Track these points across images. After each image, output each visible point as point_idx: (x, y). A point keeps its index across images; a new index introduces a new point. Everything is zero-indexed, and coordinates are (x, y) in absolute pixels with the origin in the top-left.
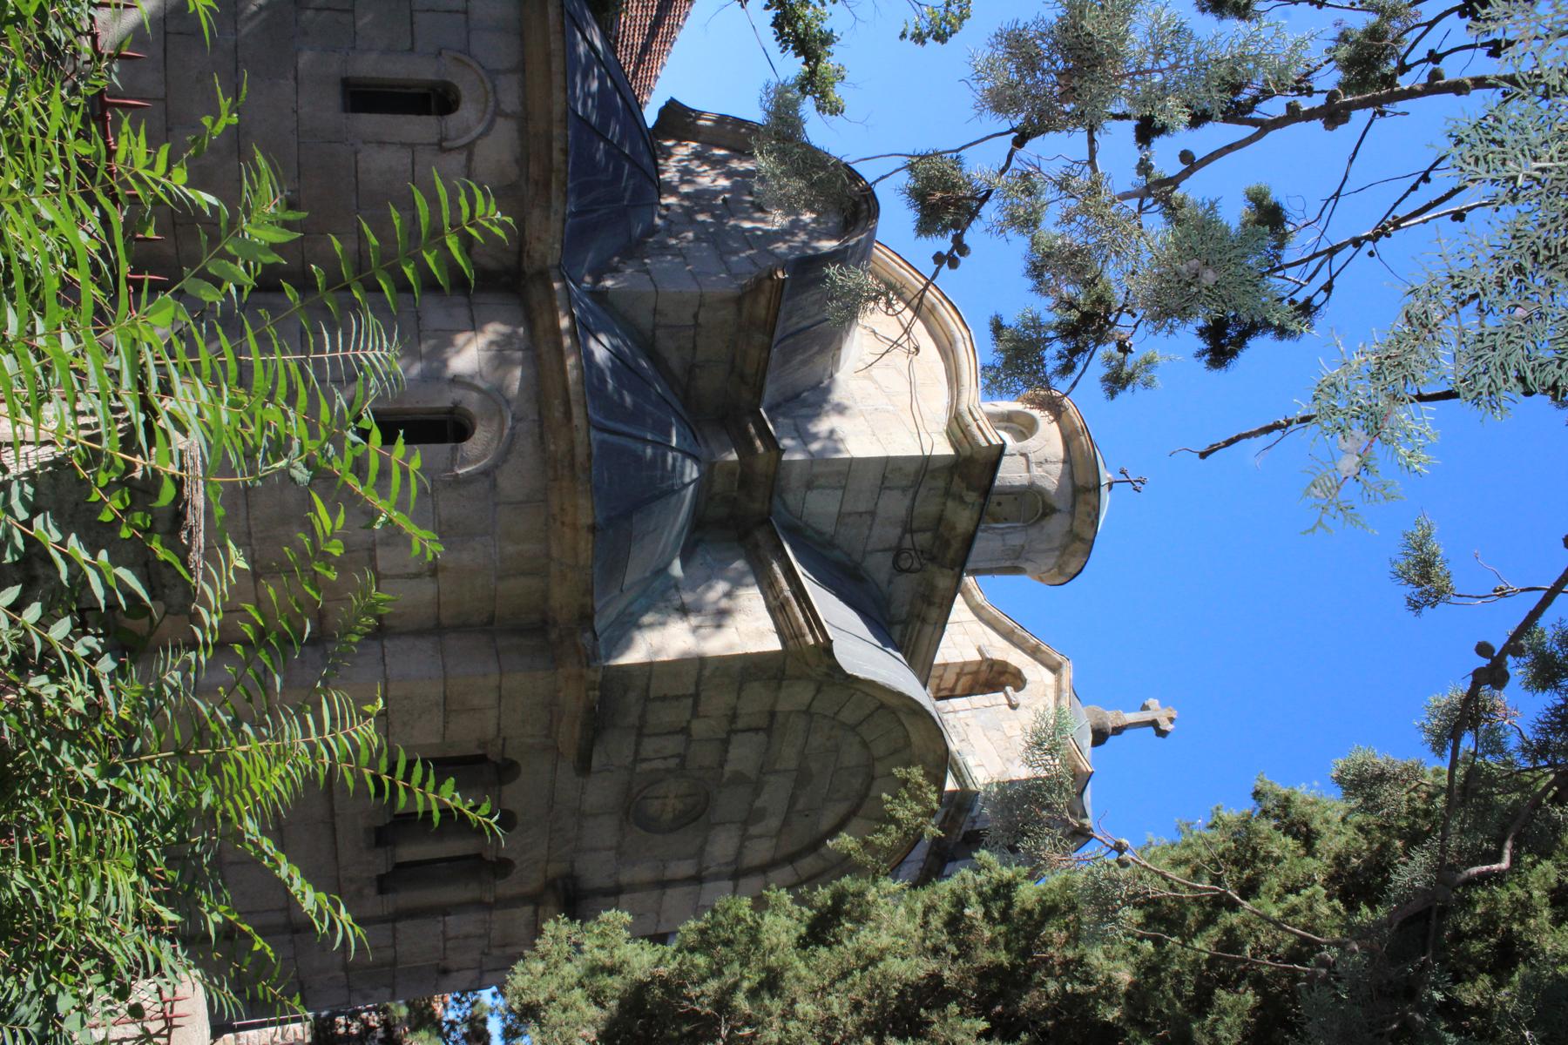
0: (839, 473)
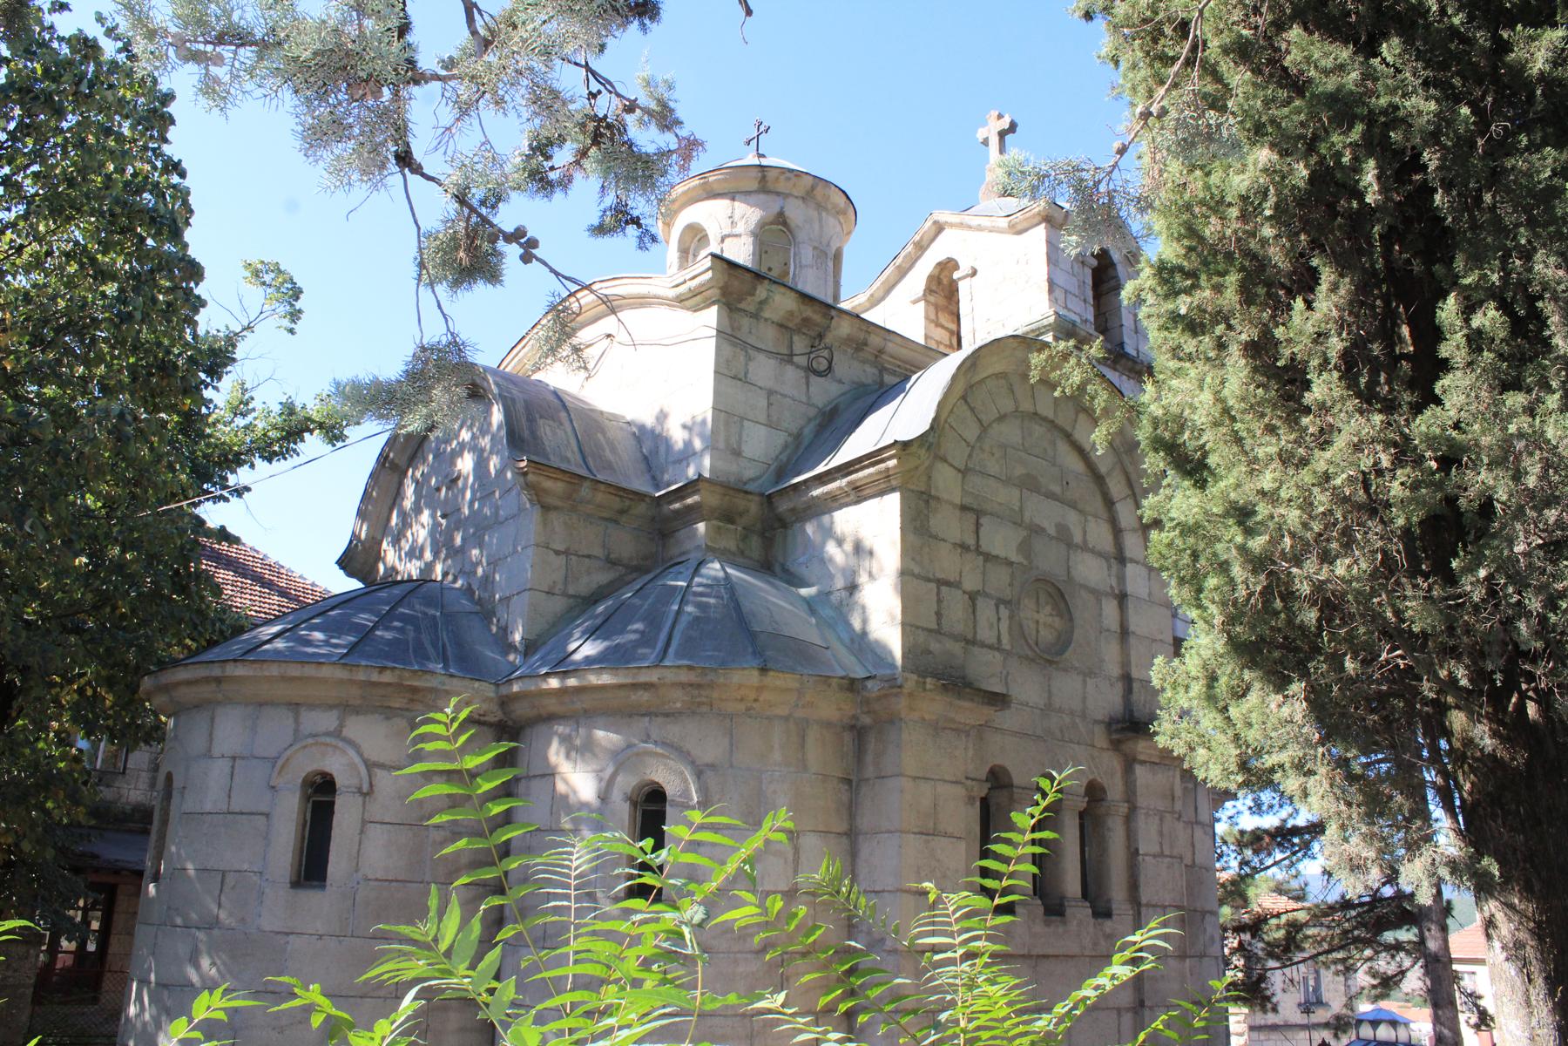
0: (727, 424)
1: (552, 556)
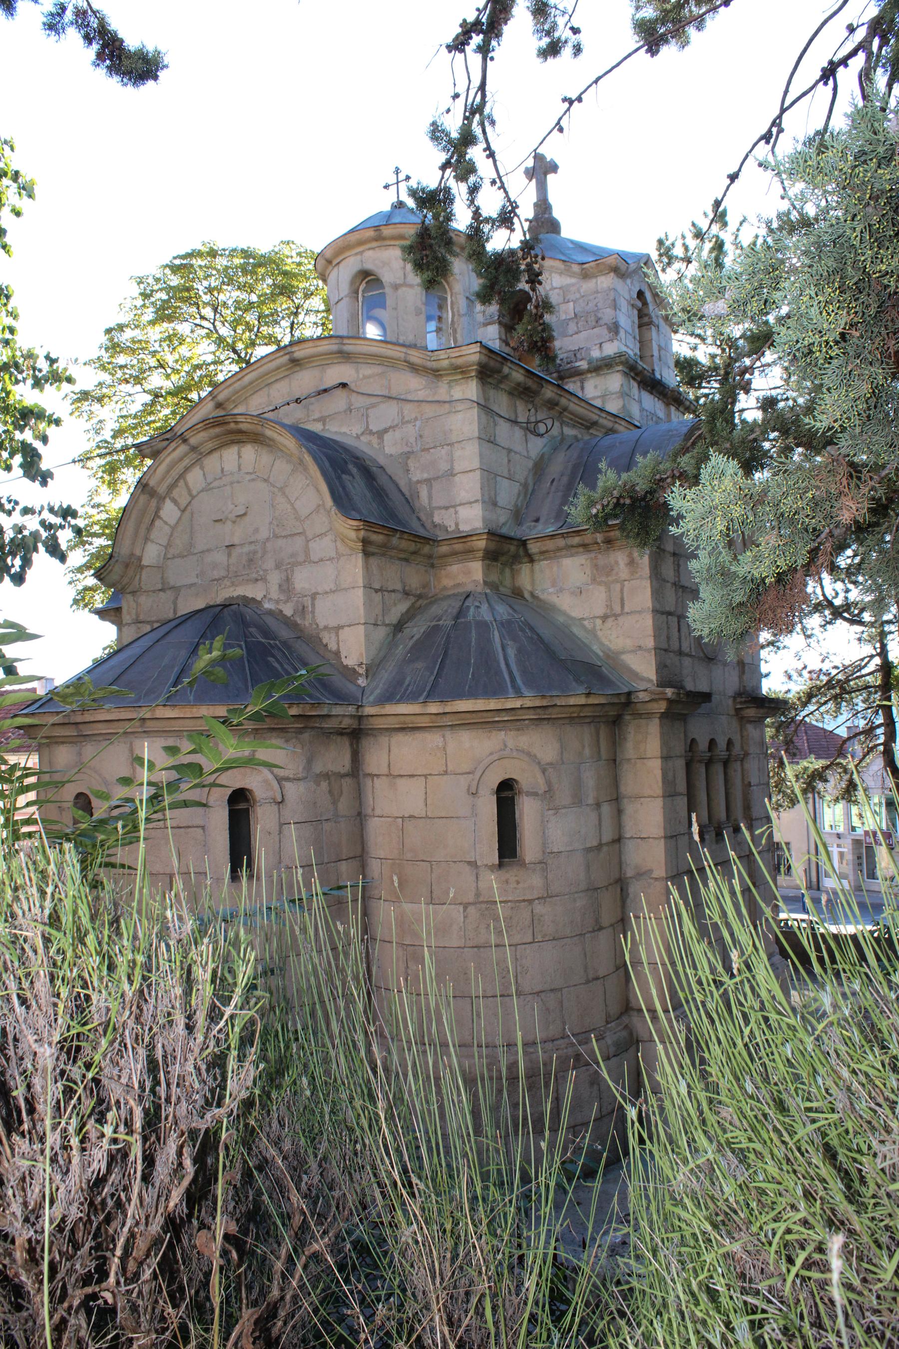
1: (374, 594)
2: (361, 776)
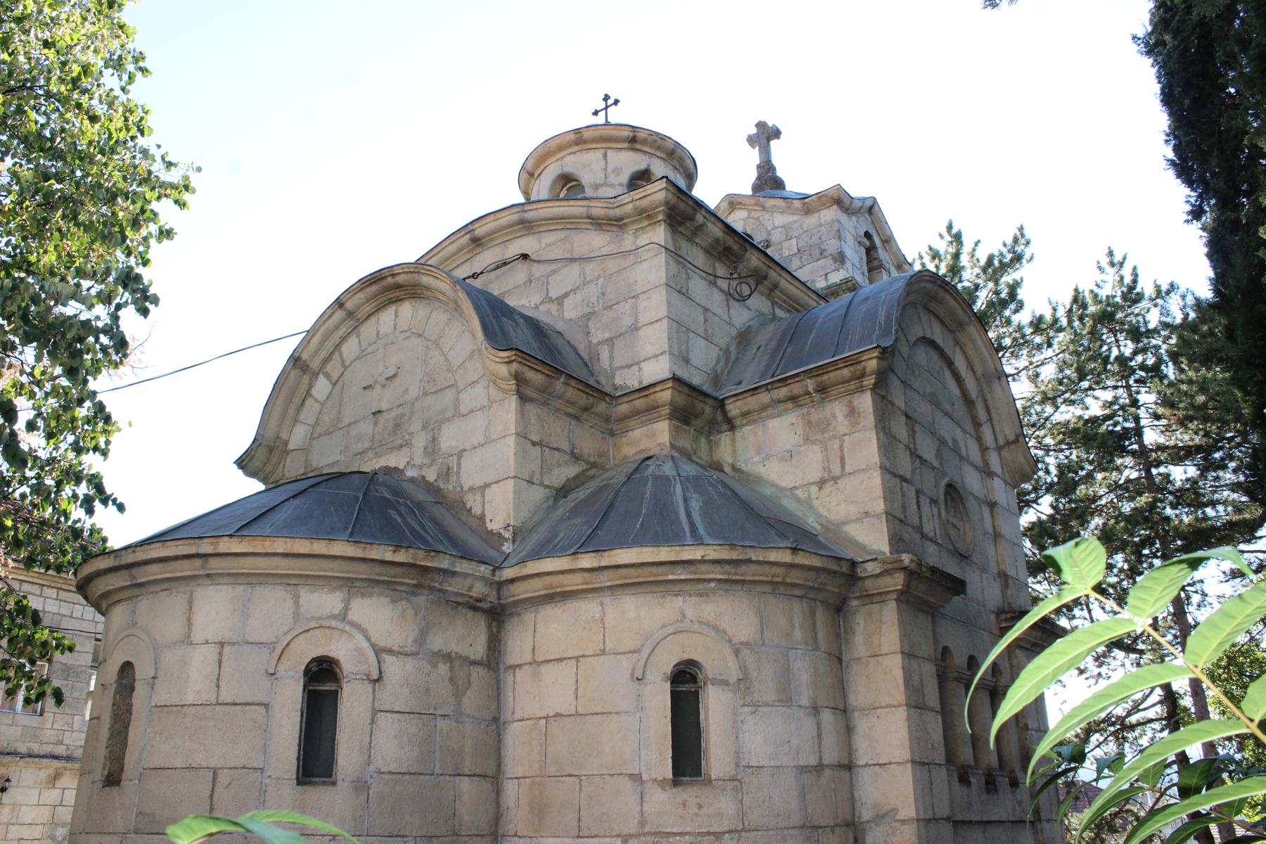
0: (678, 332)
1: (530, 447)
2: (502, 671)
